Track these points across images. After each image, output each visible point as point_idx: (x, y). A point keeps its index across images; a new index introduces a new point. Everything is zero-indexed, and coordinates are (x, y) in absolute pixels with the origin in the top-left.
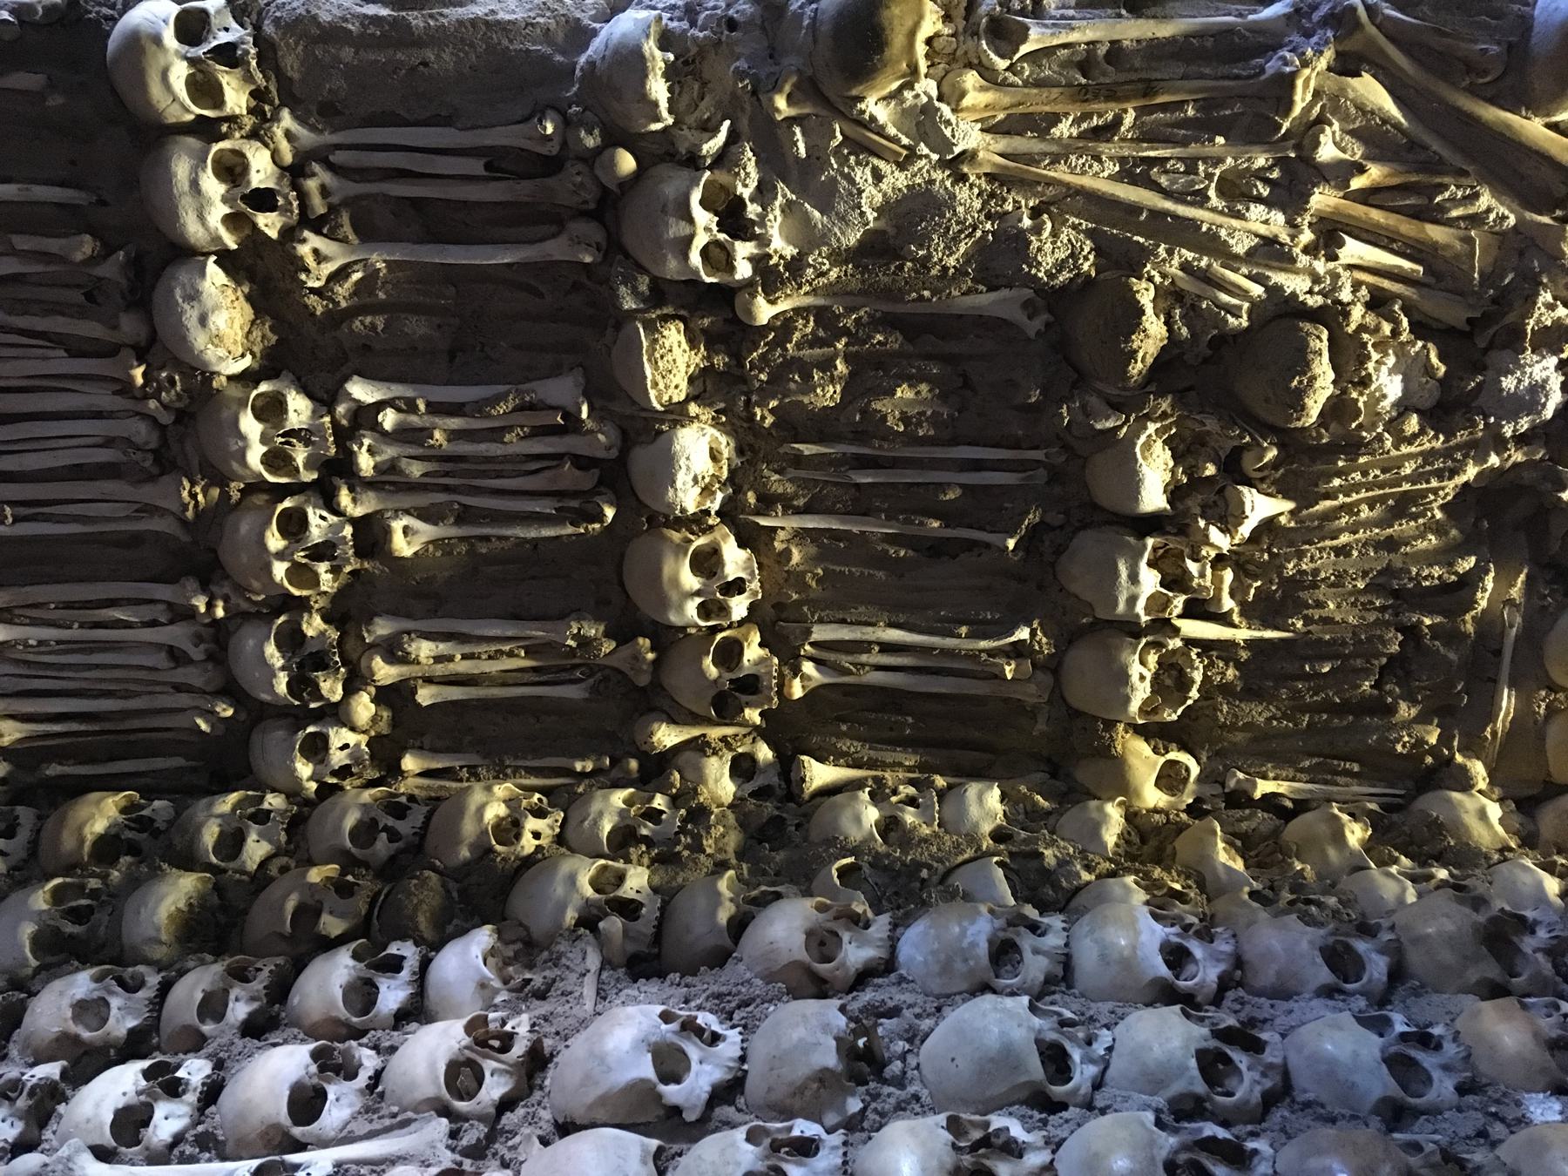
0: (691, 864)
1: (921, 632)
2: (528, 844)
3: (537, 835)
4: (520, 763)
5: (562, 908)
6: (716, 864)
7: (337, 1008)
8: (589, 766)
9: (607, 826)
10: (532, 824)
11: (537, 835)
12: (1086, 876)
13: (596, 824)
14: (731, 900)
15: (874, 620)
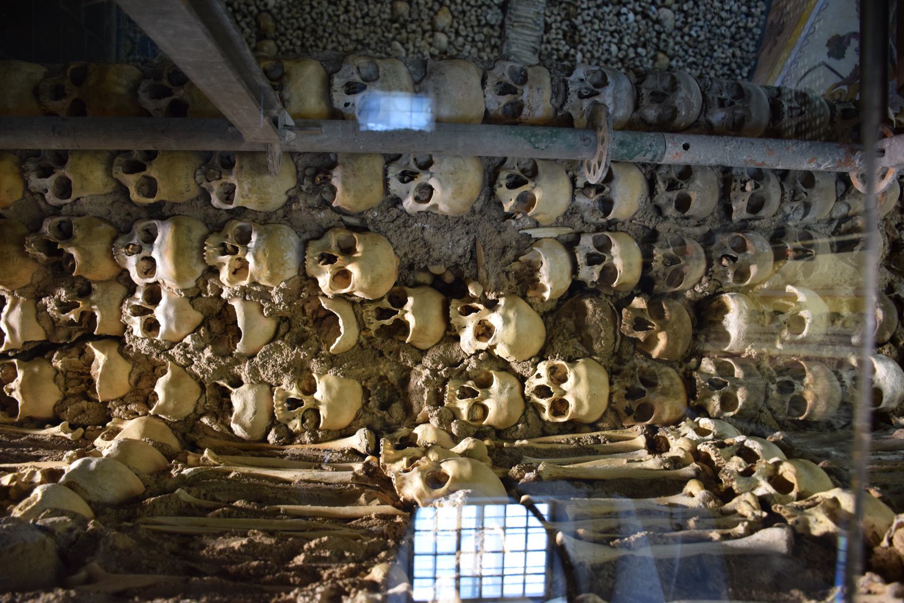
0: (436, 359)
1: (267, 478)
2: (542, 368)
3: (539, 376)
4: (566, 446)
5: (508, 307)
6: (421, 362)
7: (613, 236)
8: (518, 443)
9: (495, 386)
10: (544, 381)
11: (539, 376)
12: (188, 340)
13: (503, 385)
14: (406, 312)
15: (302, 484)
